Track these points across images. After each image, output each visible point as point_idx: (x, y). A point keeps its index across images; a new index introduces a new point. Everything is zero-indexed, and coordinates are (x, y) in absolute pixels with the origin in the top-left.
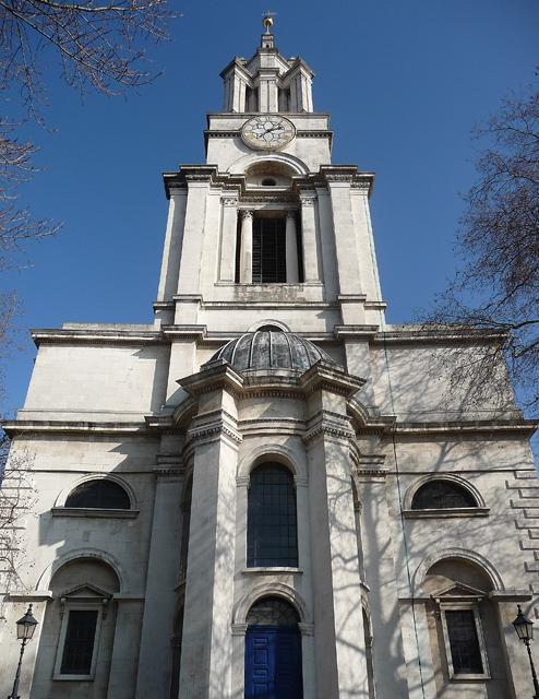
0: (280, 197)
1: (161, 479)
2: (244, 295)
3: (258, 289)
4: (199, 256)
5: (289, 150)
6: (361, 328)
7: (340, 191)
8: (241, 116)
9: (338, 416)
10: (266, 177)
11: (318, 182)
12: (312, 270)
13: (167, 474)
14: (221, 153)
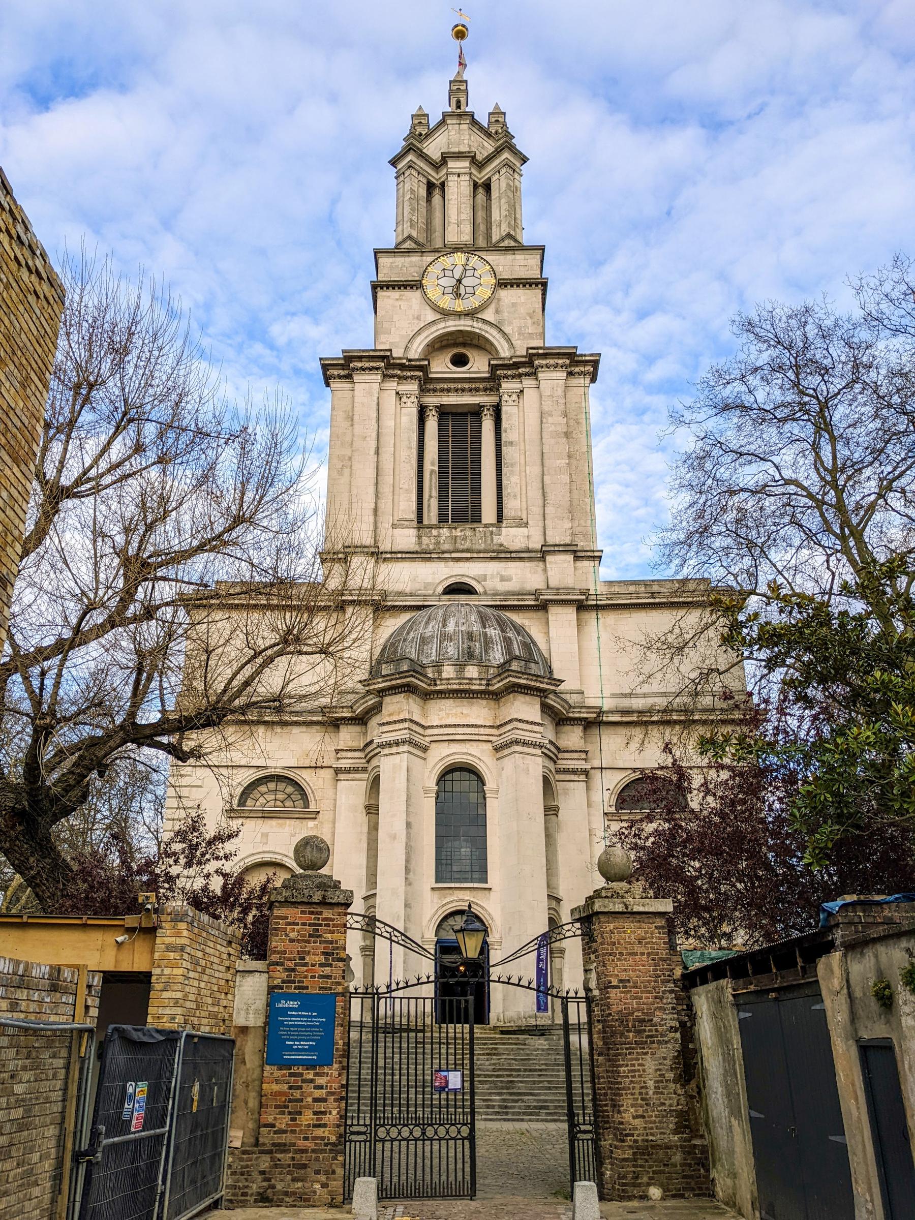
0: (472, 385)
1: (341, 776)
2: (427, 542)
3: (445, 532)
4: (372, 489)
5: (489, 315)
6: (568, 590)
9: (535, 723)
12: (511, 506)
13: (348, 771)
14: (395, 318)
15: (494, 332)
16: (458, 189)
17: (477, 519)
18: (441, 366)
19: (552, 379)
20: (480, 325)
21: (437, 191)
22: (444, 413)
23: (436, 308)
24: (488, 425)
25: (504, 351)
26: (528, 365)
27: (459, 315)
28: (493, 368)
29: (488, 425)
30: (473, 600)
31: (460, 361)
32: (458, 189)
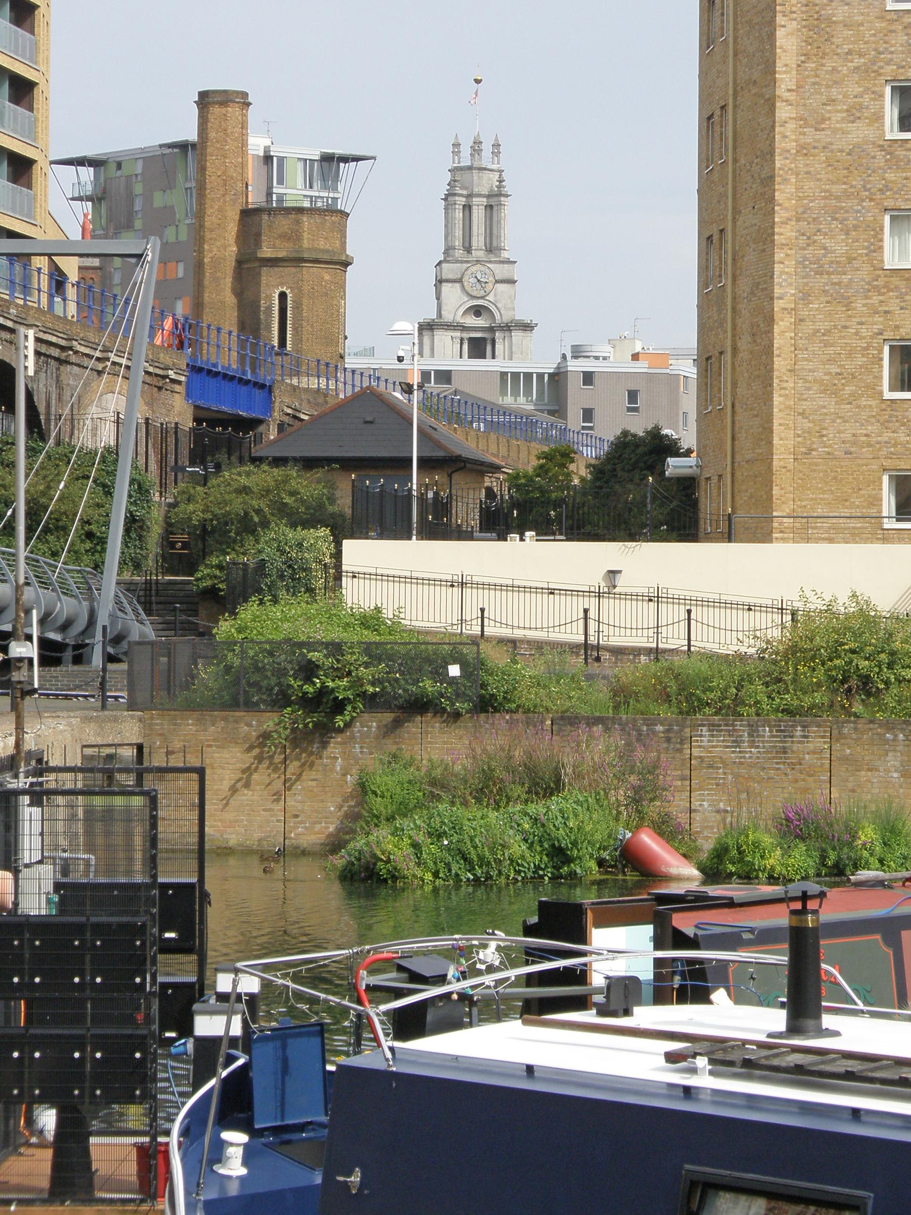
16: (478, 214)
18: (472, 321)
19: (517, 335)
22: (471, 340)
23: (468, 294)
26: (507, 328)
27: (478, 298)
32: (478, 214)
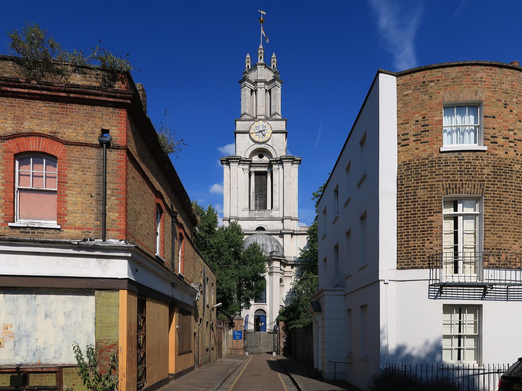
2: (252, 215)
7: (287, 165)
8: (249, 120)
10: (260, 153)
11: (280, 162)
15: (271, 149)
17: (265, 207)
18: (256, 159)
20: (267, 146)
21: (254, 92)
24: (269, 178)
25: (274, 156)
28: (270, 161)
29: (269, 178)
30: (264, 232)
31: (261, 156)
